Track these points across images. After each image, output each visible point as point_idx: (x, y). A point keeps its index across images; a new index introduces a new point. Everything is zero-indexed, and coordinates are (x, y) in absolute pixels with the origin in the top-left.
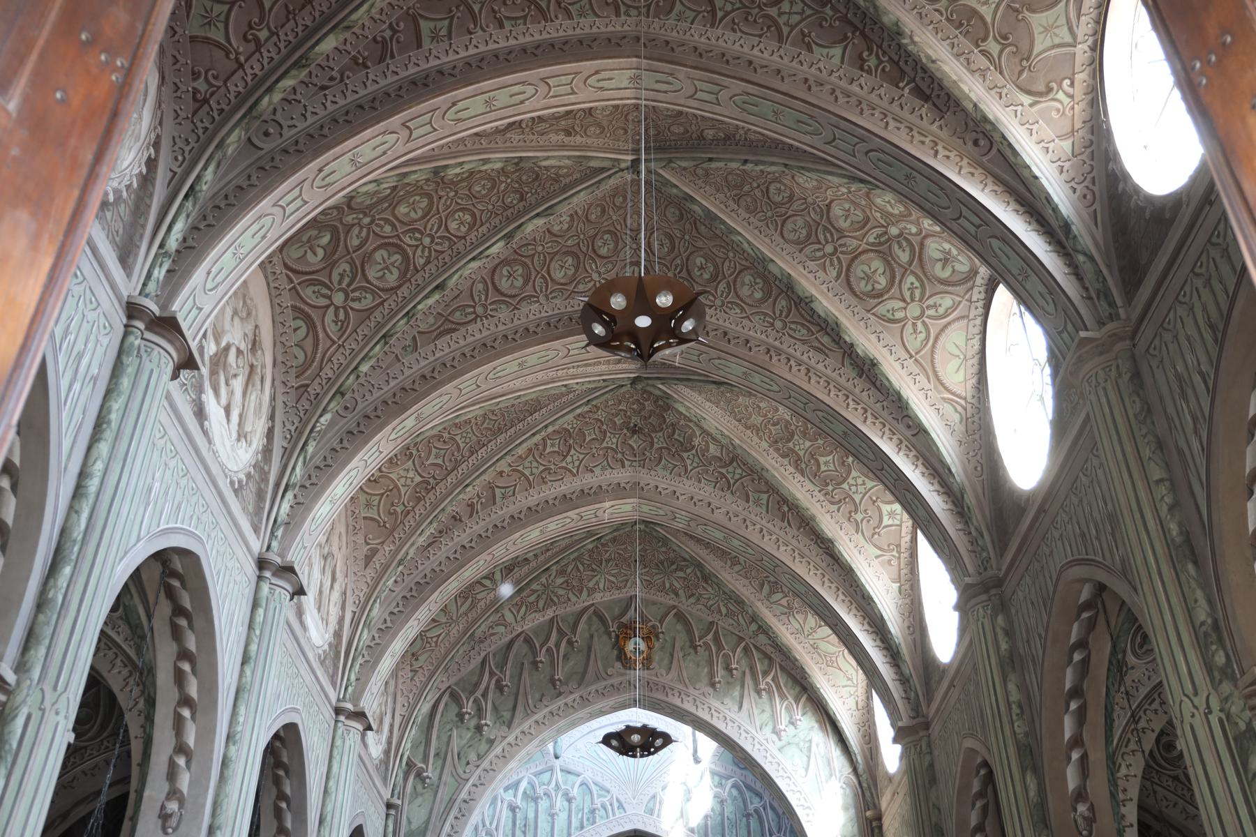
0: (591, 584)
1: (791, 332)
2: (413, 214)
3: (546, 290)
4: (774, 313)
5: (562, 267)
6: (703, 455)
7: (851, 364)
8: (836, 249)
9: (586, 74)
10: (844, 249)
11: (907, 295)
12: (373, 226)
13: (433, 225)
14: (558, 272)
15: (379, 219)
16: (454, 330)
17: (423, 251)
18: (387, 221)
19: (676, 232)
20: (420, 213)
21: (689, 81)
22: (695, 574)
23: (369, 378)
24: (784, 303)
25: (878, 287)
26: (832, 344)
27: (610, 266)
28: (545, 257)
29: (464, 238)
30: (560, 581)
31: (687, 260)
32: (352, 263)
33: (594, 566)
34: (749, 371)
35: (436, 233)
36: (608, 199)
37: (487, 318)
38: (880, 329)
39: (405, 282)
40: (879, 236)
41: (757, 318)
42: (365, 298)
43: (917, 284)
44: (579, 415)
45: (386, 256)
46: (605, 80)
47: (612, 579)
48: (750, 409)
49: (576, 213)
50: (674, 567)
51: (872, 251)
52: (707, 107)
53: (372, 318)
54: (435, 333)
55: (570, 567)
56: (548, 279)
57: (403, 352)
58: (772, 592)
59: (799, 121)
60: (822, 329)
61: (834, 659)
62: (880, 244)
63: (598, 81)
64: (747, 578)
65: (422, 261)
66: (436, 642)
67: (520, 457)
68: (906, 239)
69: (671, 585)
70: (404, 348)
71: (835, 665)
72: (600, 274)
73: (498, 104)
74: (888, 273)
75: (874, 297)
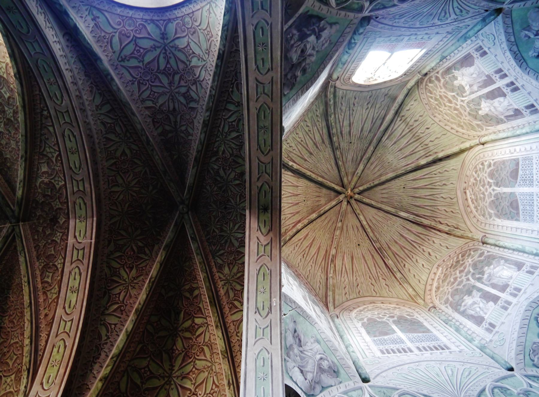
0: (236, 244)
6: (52, 175)
22: (216, 161)
30: (226, 270)
33: (223, 242)
44: (37, 258)
47: (236, 227)
48: (10, 149)
50: (219, 179)
55: (220, 261)
58: (193, 100)
61: (206, 32)
64: (193, 122)
66: (217, 386)
67: (44, 300)
69: (235, 179)
71: (208, 29)
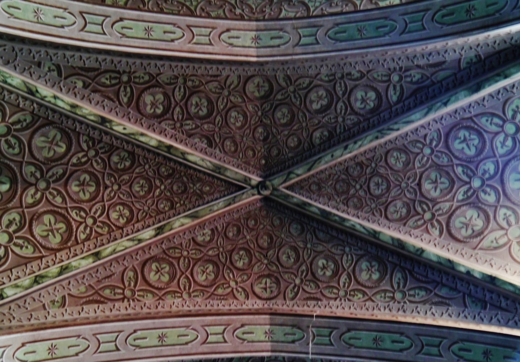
1: (412, 299)
2: (81, 194)
3: (189, 289)
4: (392, 287)
5: (204, 272)
7: (473, 302)
8: (433, 215)
9: (219, 30)
10: (441, 212)
11: (504, 224)
12: (47, 192)
13: (97, 210)
14: (200, 276)
15: (54, 189)
16: (102, 303)
17: (85, 228)
18: (59, 193)
19: (299, 244)
20: (88, 196)
21: (295, 31)
23: (11, 312)
24: (399, 275)
25: (476, 228)
26: (451, 292)
27: (245, 277)
28: (189, 261)
29: (122, 228)
31: (311, 265)
32: (22, 215)
34: (379, 334)
35: (99, 217)
36: (242, 221)
37: (133, 300)
38: (488, 258)
39: (64, 249)
40: (466, 193)
41: (378, 297)
42: (27, 247)
43: (509, 213)
45: (53, 221)
46: (233, 37)
49: (216, 228)
51: (463, 205)
52: (310, 49)
53: (29, 266)
54: (84, 300)
56: (191, 280)
57: (51, 305)
59: (378, 28)
60: (438, 283)
62: (469, 198)
63: (230, 38)
65: (83, 236)
68: (488, 186)
70: (53, 302)
72: (237, 283)
73: (154, 35)
74: (482, 215)
75: (476, 236)
